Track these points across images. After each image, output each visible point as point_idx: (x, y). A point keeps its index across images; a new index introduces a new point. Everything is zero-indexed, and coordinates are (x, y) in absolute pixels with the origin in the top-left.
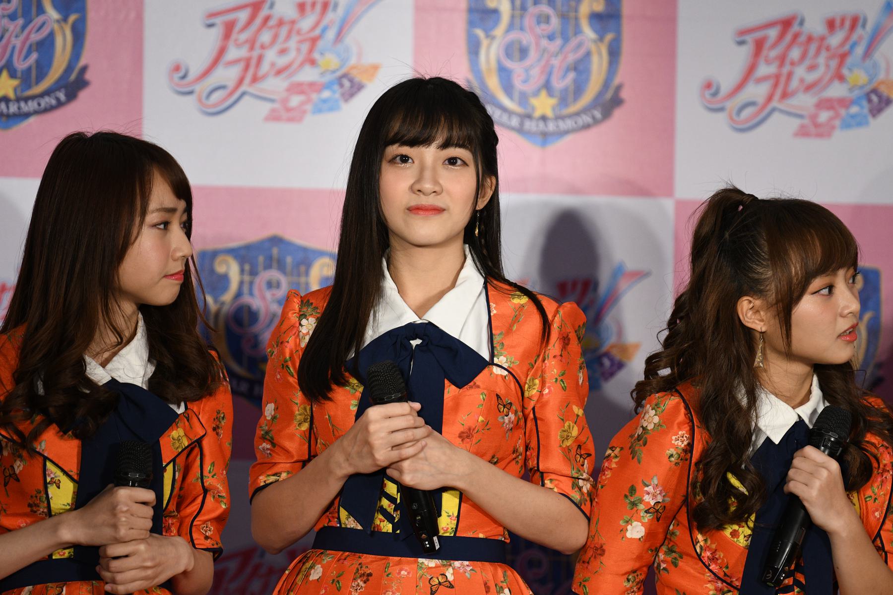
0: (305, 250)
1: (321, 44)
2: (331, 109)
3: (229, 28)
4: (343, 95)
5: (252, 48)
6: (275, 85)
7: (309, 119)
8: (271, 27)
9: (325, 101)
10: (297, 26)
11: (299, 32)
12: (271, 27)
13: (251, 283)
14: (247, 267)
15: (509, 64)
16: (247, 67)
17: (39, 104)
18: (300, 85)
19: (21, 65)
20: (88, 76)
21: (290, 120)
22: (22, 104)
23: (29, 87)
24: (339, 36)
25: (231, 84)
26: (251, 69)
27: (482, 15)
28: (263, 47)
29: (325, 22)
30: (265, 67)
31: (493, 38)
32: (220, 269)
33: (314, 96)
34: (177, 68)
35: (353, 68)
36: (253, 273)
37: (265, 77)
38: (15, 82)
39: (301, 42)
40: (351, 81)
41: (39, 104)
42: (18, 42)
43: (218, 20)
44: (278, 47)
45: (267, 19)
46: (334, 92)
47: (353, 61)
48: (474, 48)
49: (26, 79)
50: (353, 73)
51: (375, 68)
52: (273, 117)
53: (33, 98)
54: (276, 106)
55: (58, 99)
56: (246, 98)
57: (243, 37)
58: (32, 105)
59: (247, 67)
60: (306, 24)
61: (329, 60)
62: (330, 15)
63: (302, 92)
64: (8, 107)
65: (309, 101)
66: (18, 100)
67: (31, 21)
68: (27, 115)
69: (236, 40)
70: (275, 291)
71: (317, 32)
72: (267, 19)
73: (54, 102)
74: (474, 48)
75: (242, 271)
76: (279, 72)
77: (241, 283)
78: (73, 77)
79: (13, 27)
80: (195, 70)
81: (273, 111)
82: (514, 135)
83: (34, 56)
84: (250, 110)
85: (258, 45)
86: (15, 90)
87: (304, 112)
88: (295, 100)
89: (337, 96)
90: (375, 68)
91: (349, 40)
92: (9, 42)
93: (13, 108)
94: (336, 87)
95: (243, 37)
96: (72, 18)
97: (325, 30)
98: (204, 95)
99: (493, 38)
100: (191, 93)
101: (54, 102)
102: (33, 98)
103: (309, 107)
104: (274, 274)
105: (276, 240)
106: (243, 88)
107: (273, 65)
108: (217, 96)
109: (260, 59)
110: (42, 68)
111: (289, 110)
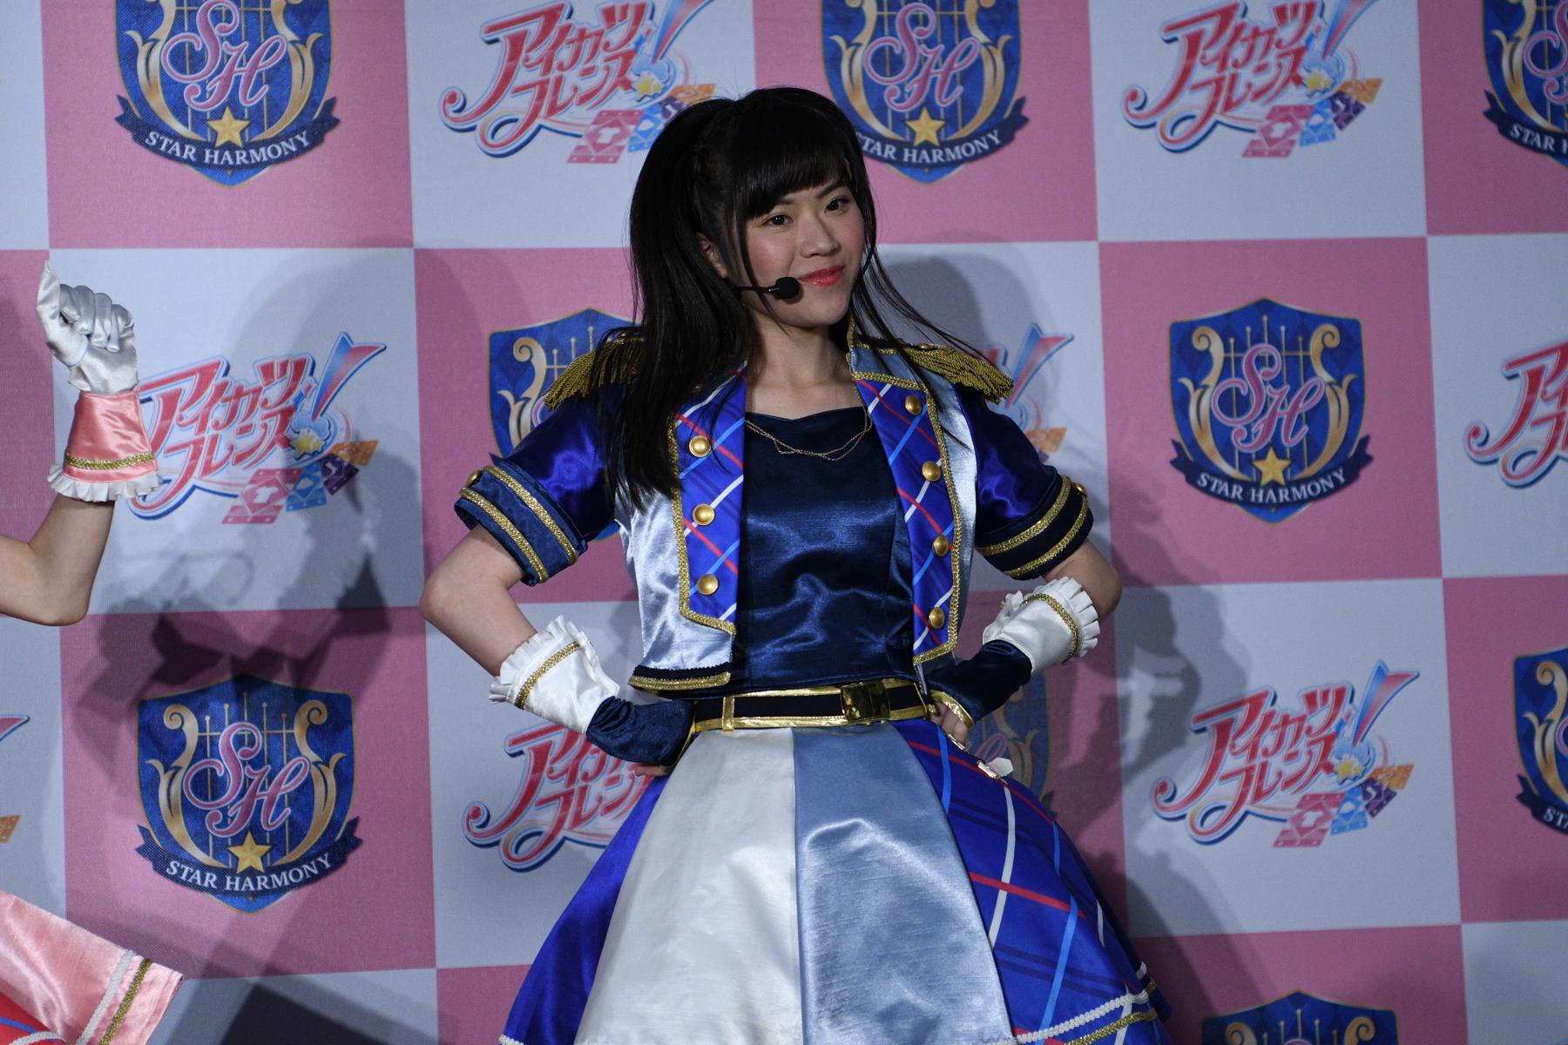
0: (1302, 314)
1: (1306, 58)
2: (1323, 138)
3: (1194, 42)
4: (1336, 120)
5: (1223, 67)
6: (1254, 111)
7: (1297, 150)
8: (1245, 40)
9: (1315, 128)
10: (1276, 37)
11: (1279, 45)
12: (1245, 40)
13: (1238, 360)
14: (1232, 341)
15: (1534, 70)
16: (1217, 92)
17: (968, 150)
18: (1284, 109)
19: (943, 103)
20: (1026, 112)
21: (1275, 154)
22: (948, 150)
23: (956, 130)
24: (1329, 48)
25: (1199, 113)
26: (1224, 95)
27: (1500, 11)
28: (1236, 65)
29: (1311, 28)
30: (1240, 89)
31: (1518, 39)
32: (1200, 345)
33: (1302, 122)
34: (1133, 96)
35: (1347, 85)
36: (1241, 347)
37: (1240, 101)
38: (939, 124)
39: (1281, 56)
40: (1346, 102)
41: (968, 150)
42: (937, 74)
43: (1179, 34)
44: (1254, 63)
45: (1239, 30)
46: (1326, 116)
47: (1347, 76)
48: (1493, 54)
49: (951, 121)
50: (1349, 90)
51: (1375, 84)
52: (1253, 151)
53: (960, 142)
54: (1257, 137)
55: (990, 142)
56: (1219, 127)
57: (1211, 53)
58: (959, 152)
59: (1217, 92)
60: (1287, 33)
61: (1317, 76)
62: (1316, 20)
63: (1288, 119)
64: (931, 156)
65: (1296, 128)
66: (943, 145)
67: (954, 46)
68: (955, 164)
69: (1203, 57)
70: (1265, 369)
71: (1302, 42)
72: (1239, 30)
73: (986, 147)
74: (1493, 54)
75: (1227, 349)
76: (1257, 95)
77: (1227, 361)
78: (1007, 114)
79: (932, 54)
80: (1154, 101)
81: (1253, 143)
82: (1550, 159)
83: (960, 89)
84: (1225, 144)
85: (1230, 62)
86: (938, 133)
87: (1292, 143)
88: (1279, 129)
89: (1331, 121)
90: (1375, 84)
91: (1340, 51)
92: (928, 74)
93: (937, 156)
94: (1329, 110)
95: (1211, 53)
96: (1004, 39)
97: (1311, 38)
98: (1170, 125)
99: (1518, 39)
100: (1153, 125)
101: (986, 147)
102: (960, 142)
103: (1296, 137)
104: (1266, 349)
105: (1265, 306)
106: (1216, 117)
107: (1249, 86)
108: (1182, 129)
109: (1234, 78)
110: (969, 106)
111: (1271, 141)
